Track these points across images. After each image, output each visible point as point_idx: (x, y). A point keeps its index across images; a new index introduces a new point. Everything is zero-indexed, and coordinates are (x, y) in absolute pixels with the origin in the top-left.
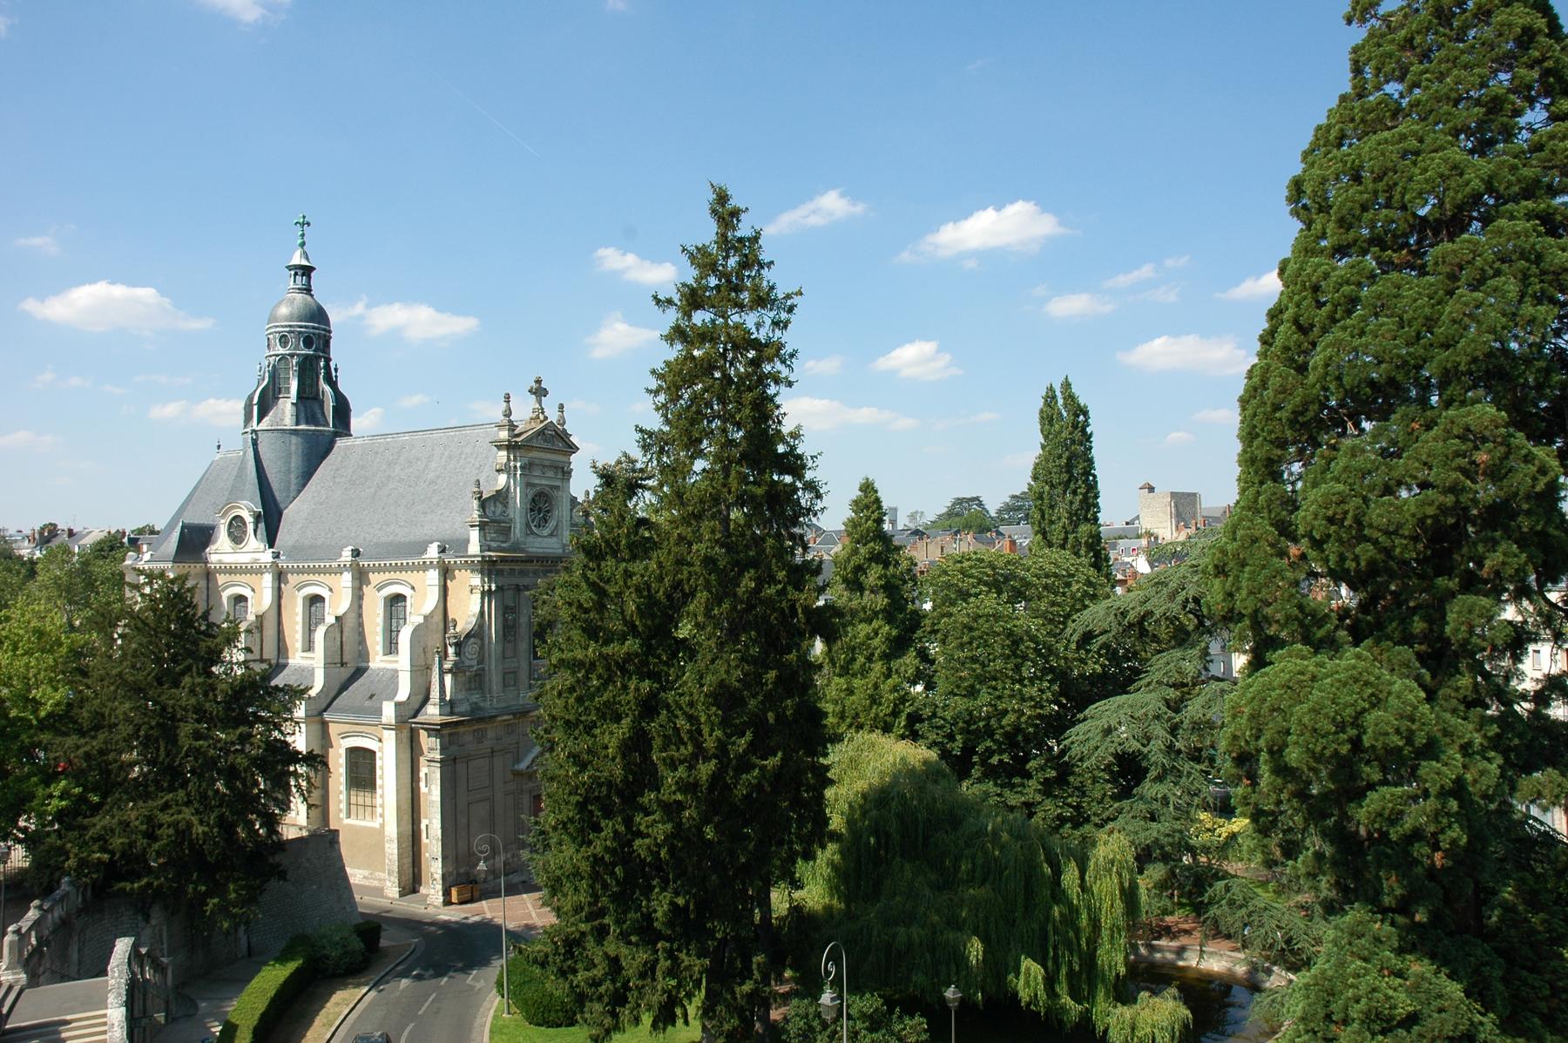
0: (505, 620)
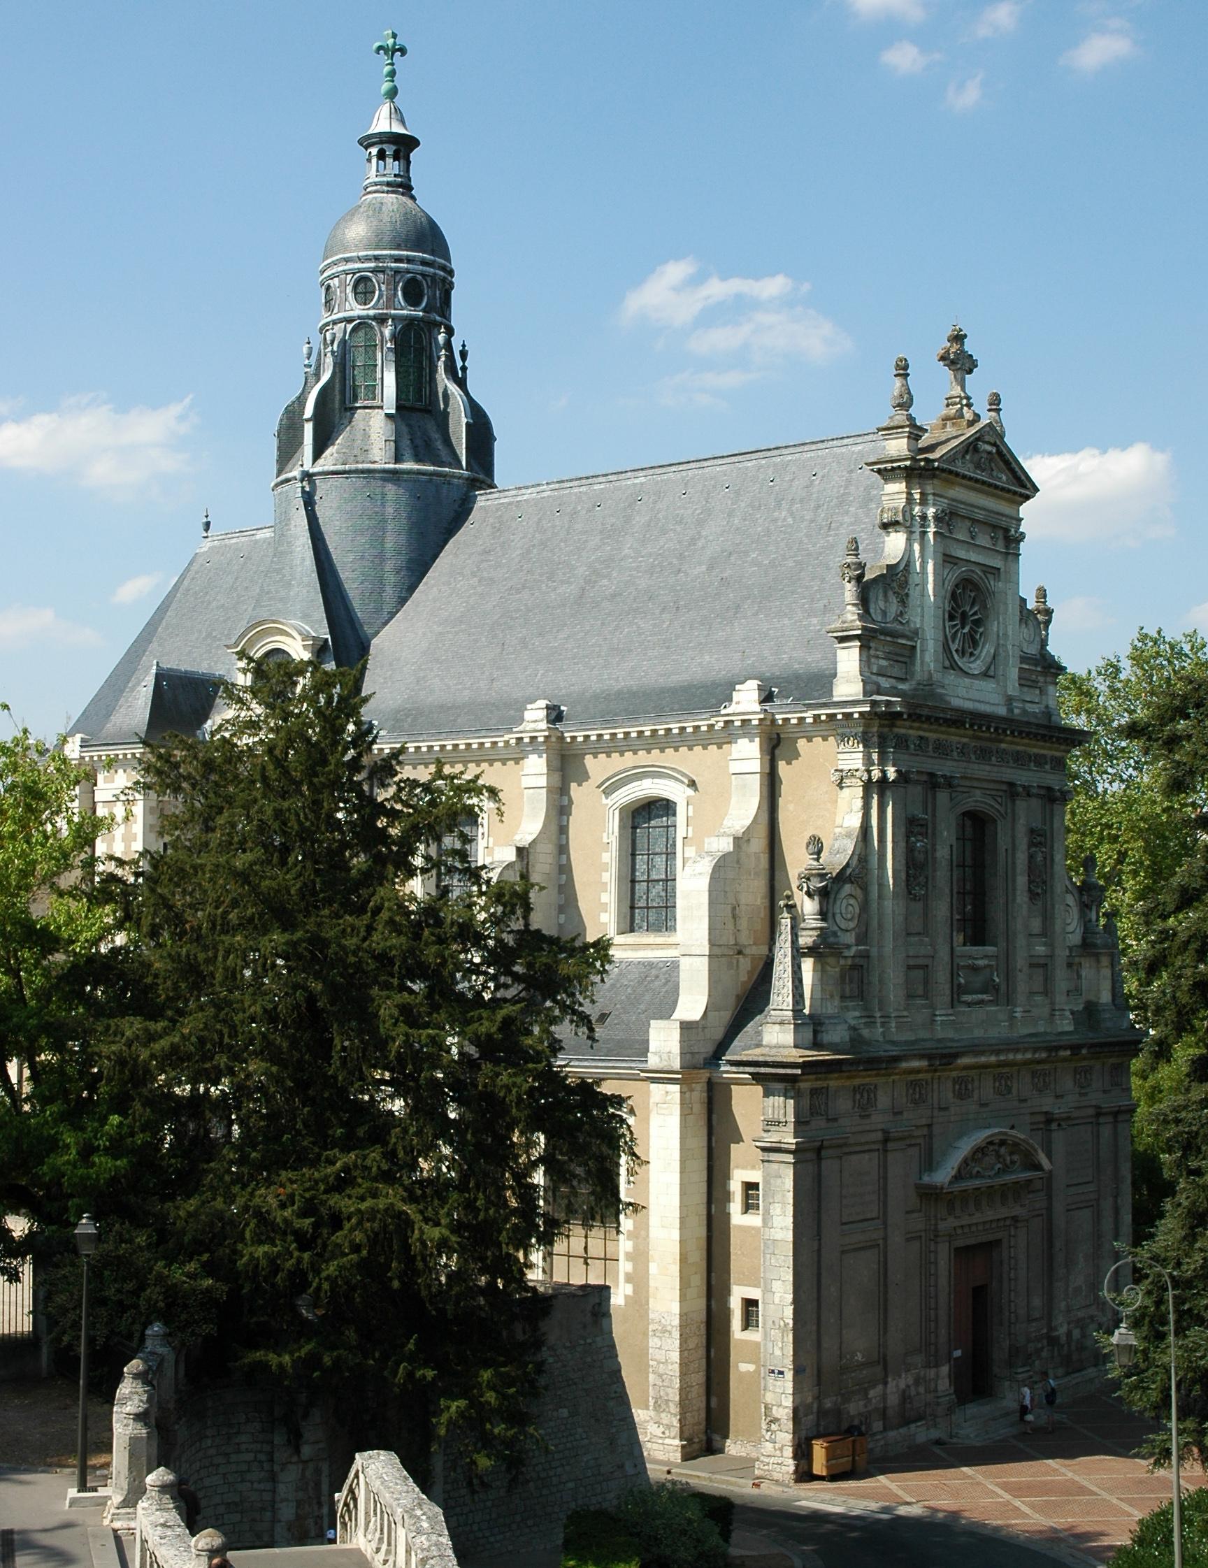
0: (910, 850)
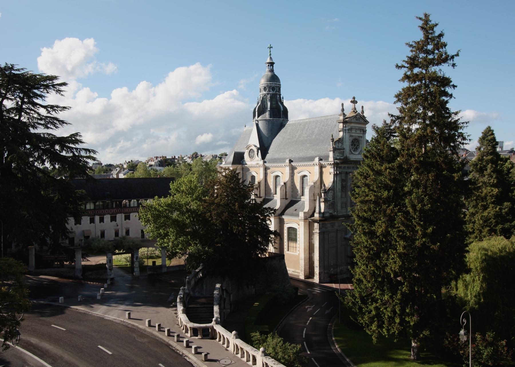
0: (342, 184)
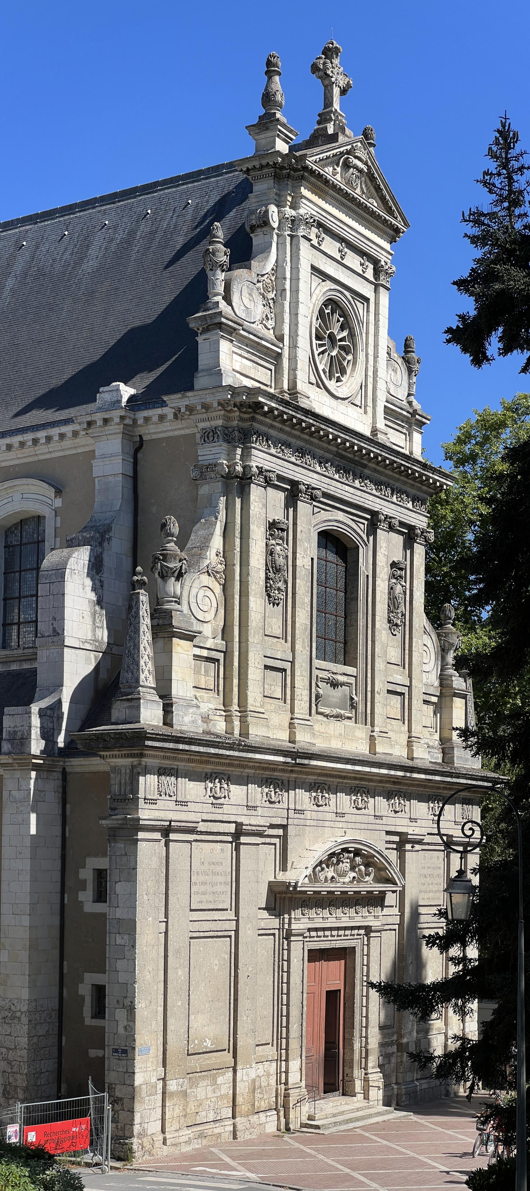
0: (270, 553)
